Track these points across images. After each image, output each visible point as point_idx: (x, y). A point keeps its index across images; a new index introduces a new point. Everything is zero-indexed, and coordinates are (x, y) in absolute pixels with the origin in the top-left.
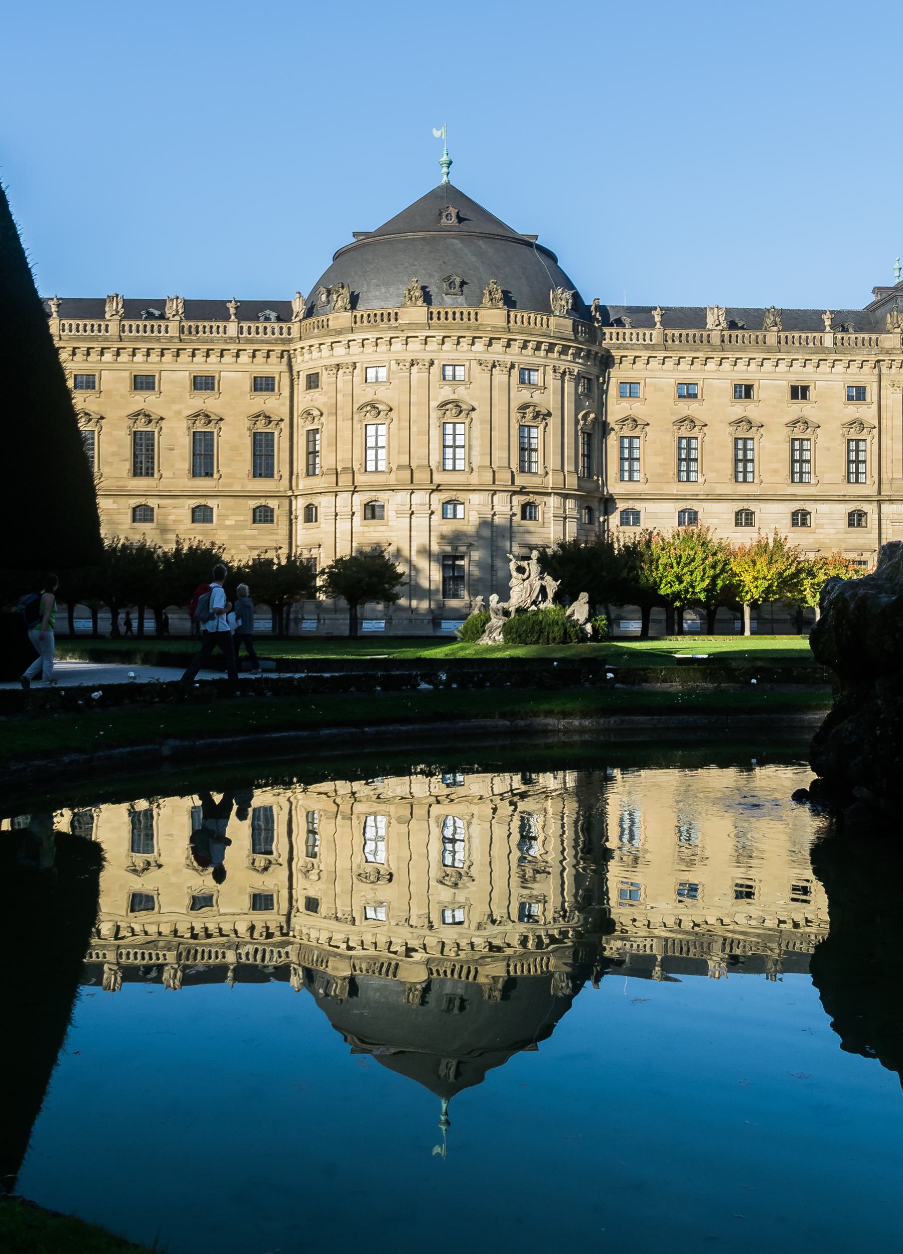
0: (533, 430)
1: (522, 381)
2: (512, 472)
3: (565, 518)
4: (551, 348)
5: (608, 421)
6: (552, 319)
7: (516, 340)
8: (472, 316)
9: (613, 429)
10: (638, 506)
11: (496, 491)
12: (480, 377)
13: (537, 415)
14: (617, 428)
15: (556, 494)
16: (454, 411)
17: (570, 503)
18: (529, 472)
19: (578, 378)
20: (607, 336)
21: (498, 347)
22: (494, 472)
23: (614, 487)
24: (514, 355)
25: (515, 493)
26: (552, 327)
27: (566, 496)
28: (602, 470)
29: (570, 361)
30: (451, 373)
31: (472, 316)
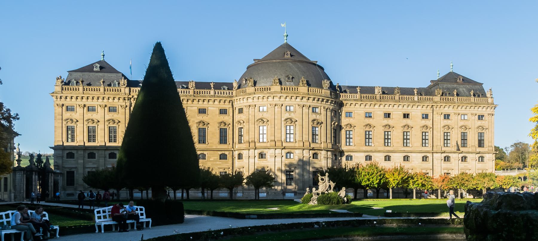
10: (352, 154)
12: (299, 110)
13: (318, 123)
14: (345, 127)
17: (329, 153)
21: (305, 100)
23: (344, 148)
24: (310, 102)
27: (328, 151)
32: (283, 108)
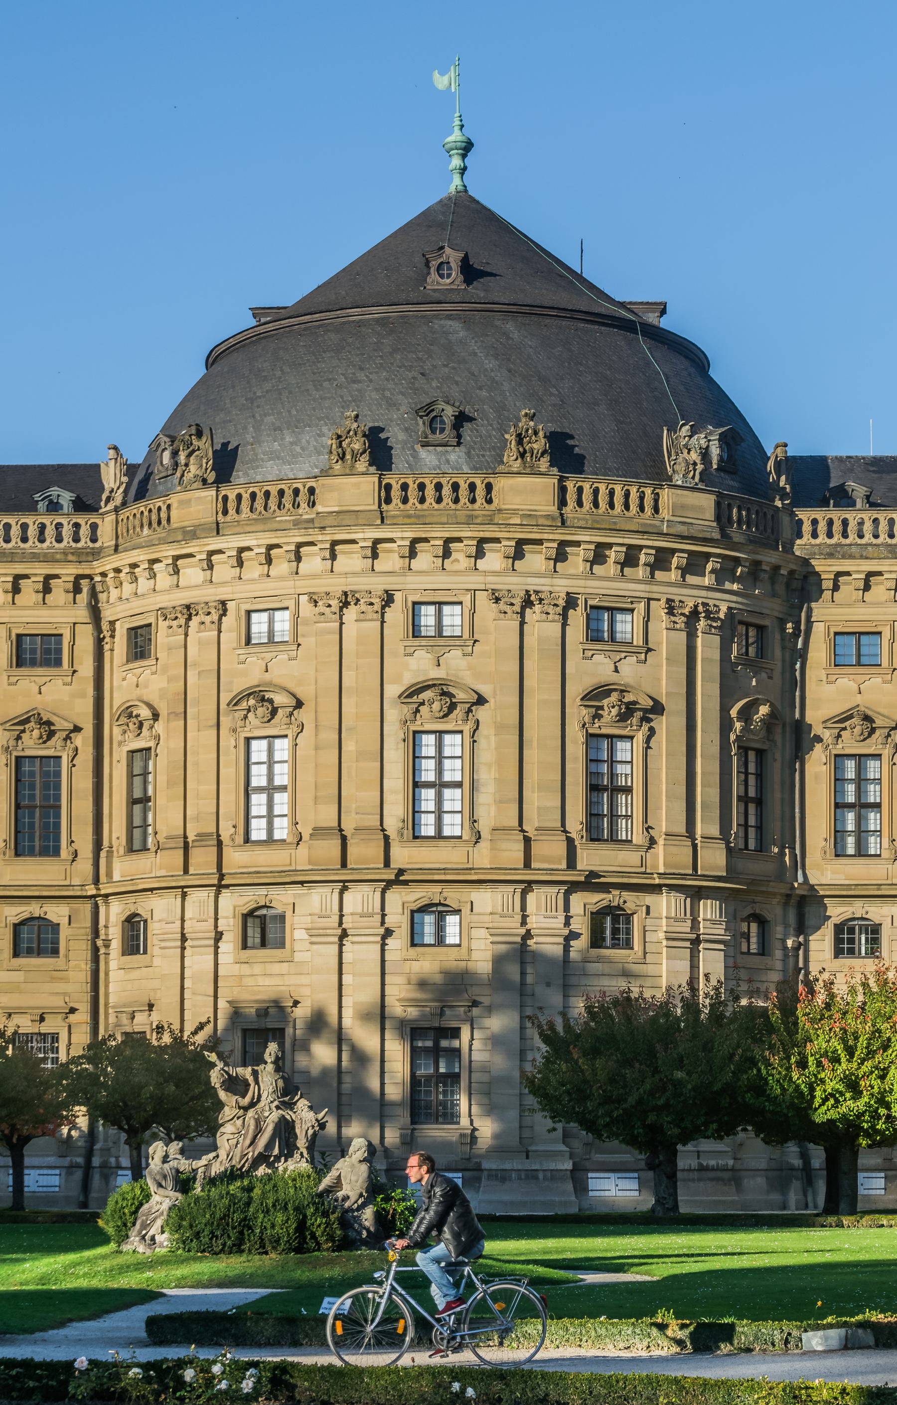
0: (620, 745)
1: (594, 636)
2: (570, 842)
3: (696, 942)
4: (661, 560)
5: (809, 719)
6: (666, 495)
7: (577, 544)
8: (480, 492)
9: (818, 739)
11: (530, 883)
12: (497, 628)
13: (628, 711)
14: (827, 735)
15: (672, 888)
16: (436, 706)
17: (708, 909)
18: (613, 839)
19: (730, 627)
20: (807, 528)
22: (527, 841)
23: (823, 870)
24: (574, 578)
25: (573, 887)
26: (665, 513)
27: (696, 894)
28: (792, 832)
29: (708, 589)
30: (431, 621)
31: (480, 492)
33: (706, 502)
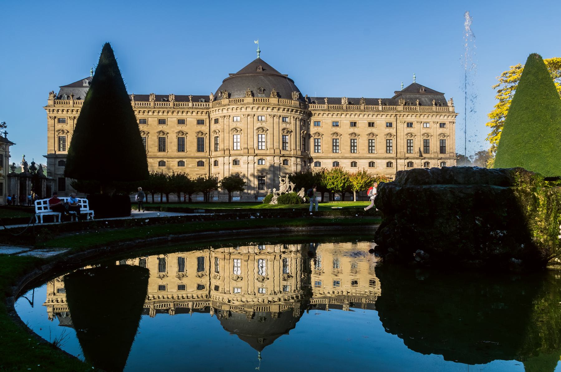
4: (292, 111)
10: (320, 160)
12: (270, 120)
17: (299, 160)
21: (275, 110)
23: (313, 155)
24: (280, 112)
25: (281, 156)
27: (297, 158)
28: (308, 149)
32: (256, 117)
33: (298, 102)
